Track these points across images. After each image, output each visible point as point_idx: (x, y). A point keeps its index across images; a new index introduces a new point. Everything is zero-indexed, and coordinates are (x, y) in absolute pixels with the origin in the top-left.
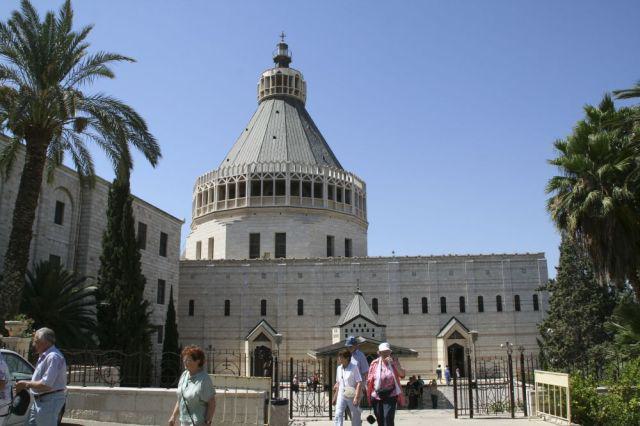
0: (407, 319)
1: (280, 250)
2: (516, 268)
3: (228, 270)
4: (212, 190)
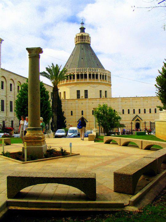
3: (72, 102)
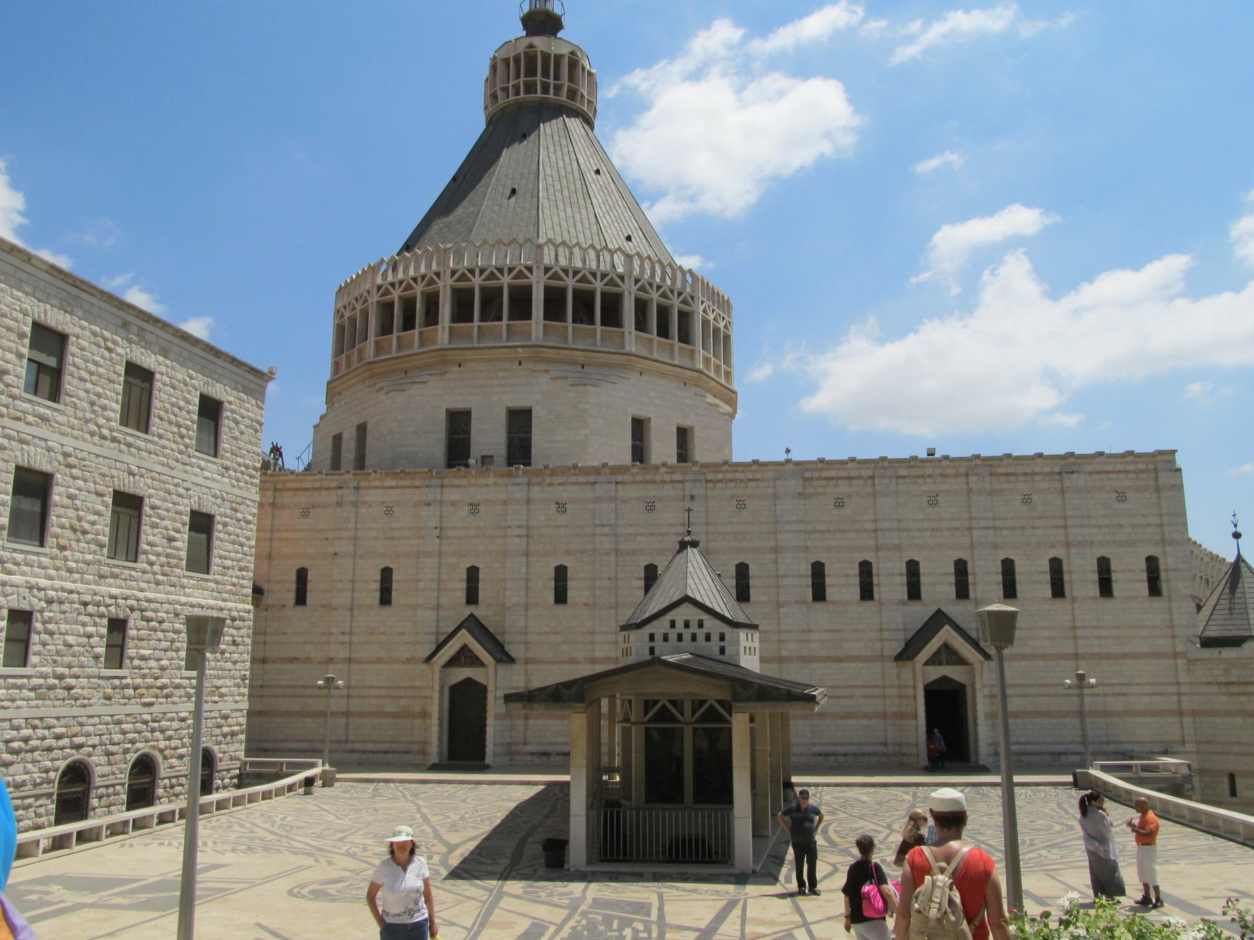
3: (392, 496)
4: (365, 313)
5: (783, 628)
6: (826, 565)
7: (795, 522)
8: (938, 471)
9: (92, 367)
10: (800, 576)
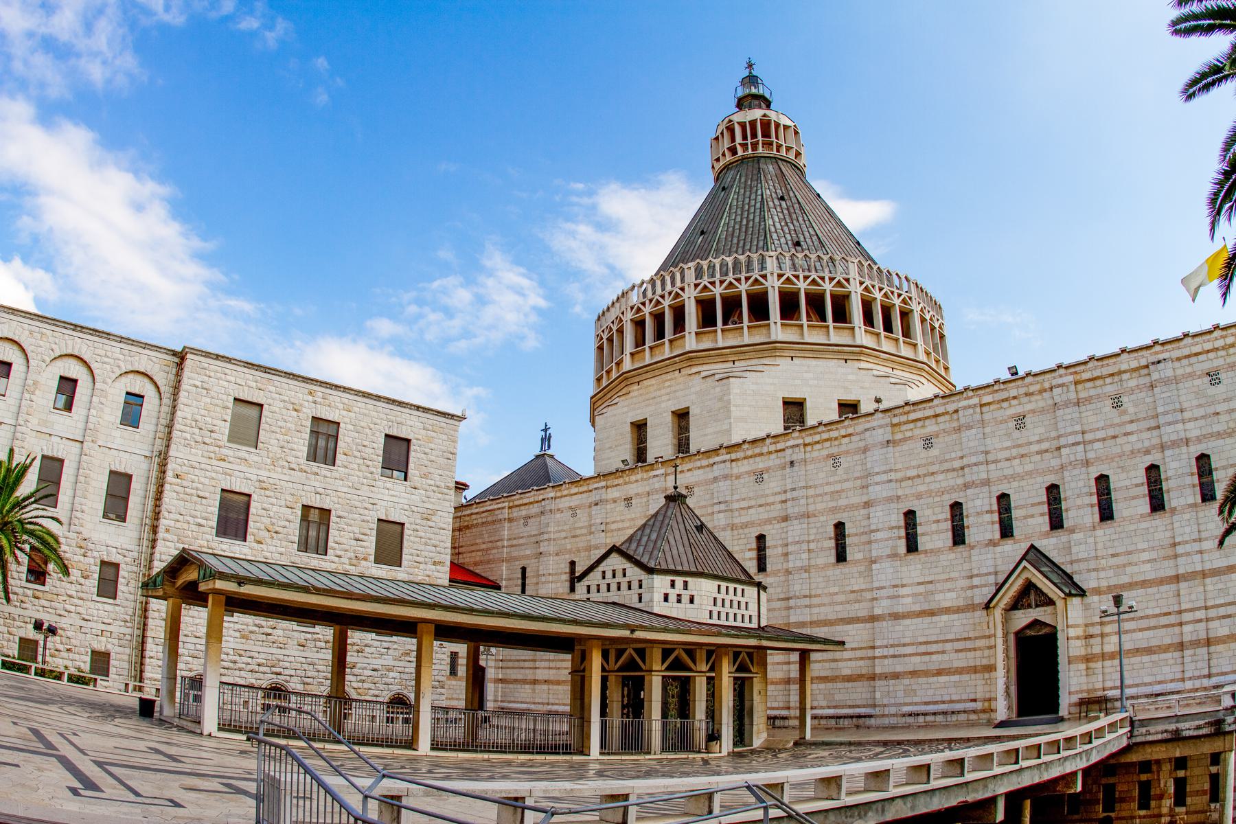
0: (914, 568)
1: (683, 445)
2: (1191, 376)
5: (876, 585)
6: (918, 514)
7: (885, 472)
8: (1022, 391)
9: (280, 423)
10: (893, 528)
